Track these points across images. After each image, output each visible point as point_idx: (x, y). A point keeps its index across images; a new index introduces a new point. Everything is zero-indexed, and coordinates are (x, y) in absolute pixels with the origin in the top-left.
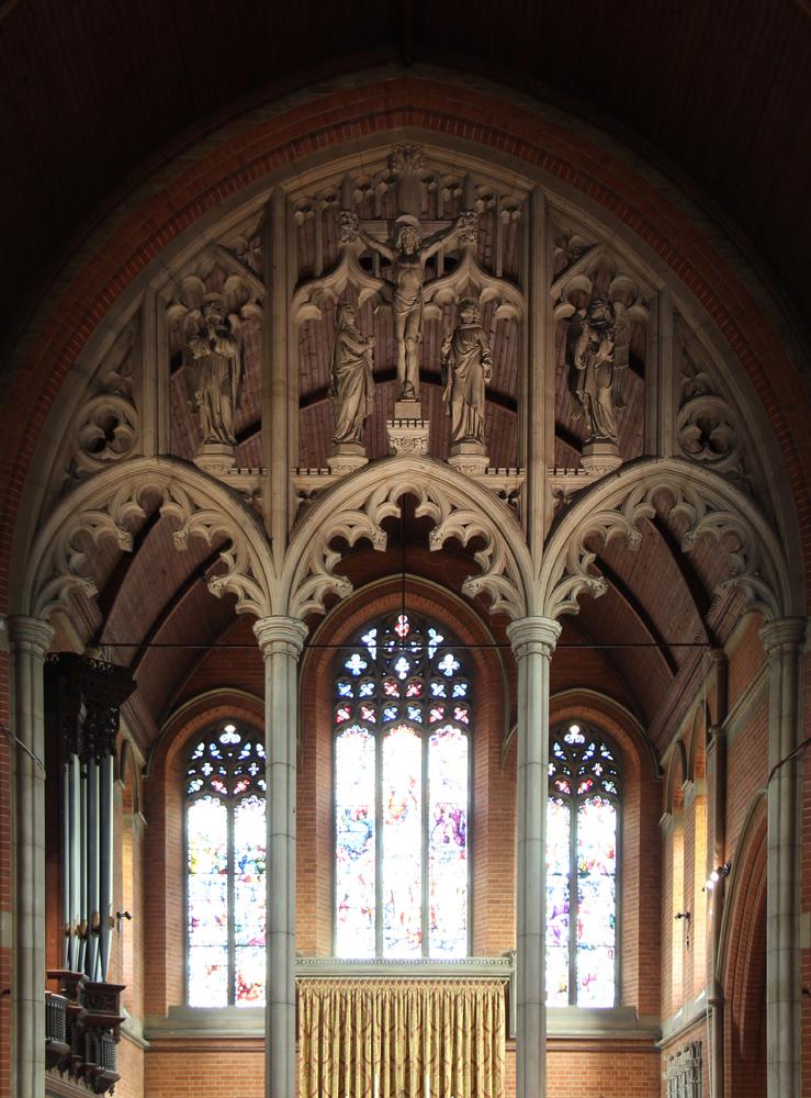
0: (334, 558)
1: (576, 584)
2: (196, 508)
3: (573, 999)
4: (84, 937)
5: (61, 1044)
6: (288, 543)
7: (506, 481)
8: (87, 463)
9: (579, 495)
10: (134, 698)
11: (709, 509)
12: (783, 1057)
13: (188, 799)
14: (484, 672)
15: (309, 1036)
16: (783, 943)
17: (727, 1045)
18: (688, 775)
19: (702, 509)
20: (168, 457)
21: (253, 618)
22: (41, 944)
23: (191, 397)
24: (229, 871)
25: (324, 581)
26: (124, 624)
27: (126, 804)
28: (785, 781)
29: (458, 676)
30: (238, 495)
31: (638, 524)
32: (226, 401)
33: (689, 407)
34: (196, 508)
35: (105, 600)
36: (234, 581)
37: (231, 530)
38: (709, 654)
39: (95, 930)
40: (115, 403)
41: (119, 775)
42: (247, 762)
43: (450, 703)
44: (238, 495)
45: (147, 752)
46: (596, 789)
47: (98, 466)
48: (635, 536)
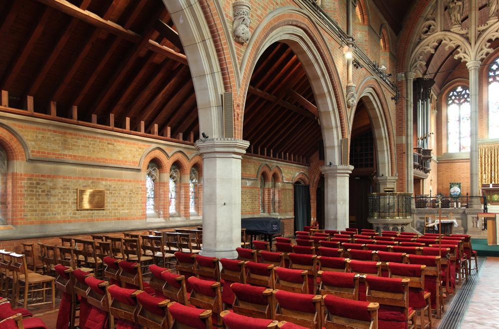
0: (489, 44)
2: (451, 40)
4: (422, 139)
5: (417, 163)
6: (475, 43)
8: (423, 36)
10: (435, 85)
13: (448, 105)
15: (481, 158)
20: (444, 30)
21: (467, 62)
22: (412, 142)
23: (450, 16)
24: (459, 120)
25: (486, 50)
26: (432, 69)
27: (432, 108)
30: (462, 35)
32: (459, 15)
34: (451, 40)
35: (427, 65)
36: (461, 55)
37: (460, 43)
39: (425, 138)
40: (431, 22)
41: (431, 102)
42: (464, 95)
44: (462, 35)
45: (438, 96)
47: (426, 36)
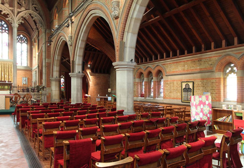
1: (21, 21)
3: (21, 65)
7: (12, 9)
9: (20, 12)
11: (36, 16)
12: (44, 73)
14: (10, 27)
16: (44, 61)
17: (39, 71)
18: (35, 42)
19: (35, 16)
28: (44, 45)
29: (6, 27)
31: (28, 16)
33: (33, 5)
38: (37, 30)
43: (5, 30)
46: (24, 42)
48: (27, 17)
